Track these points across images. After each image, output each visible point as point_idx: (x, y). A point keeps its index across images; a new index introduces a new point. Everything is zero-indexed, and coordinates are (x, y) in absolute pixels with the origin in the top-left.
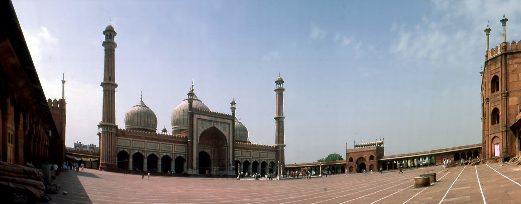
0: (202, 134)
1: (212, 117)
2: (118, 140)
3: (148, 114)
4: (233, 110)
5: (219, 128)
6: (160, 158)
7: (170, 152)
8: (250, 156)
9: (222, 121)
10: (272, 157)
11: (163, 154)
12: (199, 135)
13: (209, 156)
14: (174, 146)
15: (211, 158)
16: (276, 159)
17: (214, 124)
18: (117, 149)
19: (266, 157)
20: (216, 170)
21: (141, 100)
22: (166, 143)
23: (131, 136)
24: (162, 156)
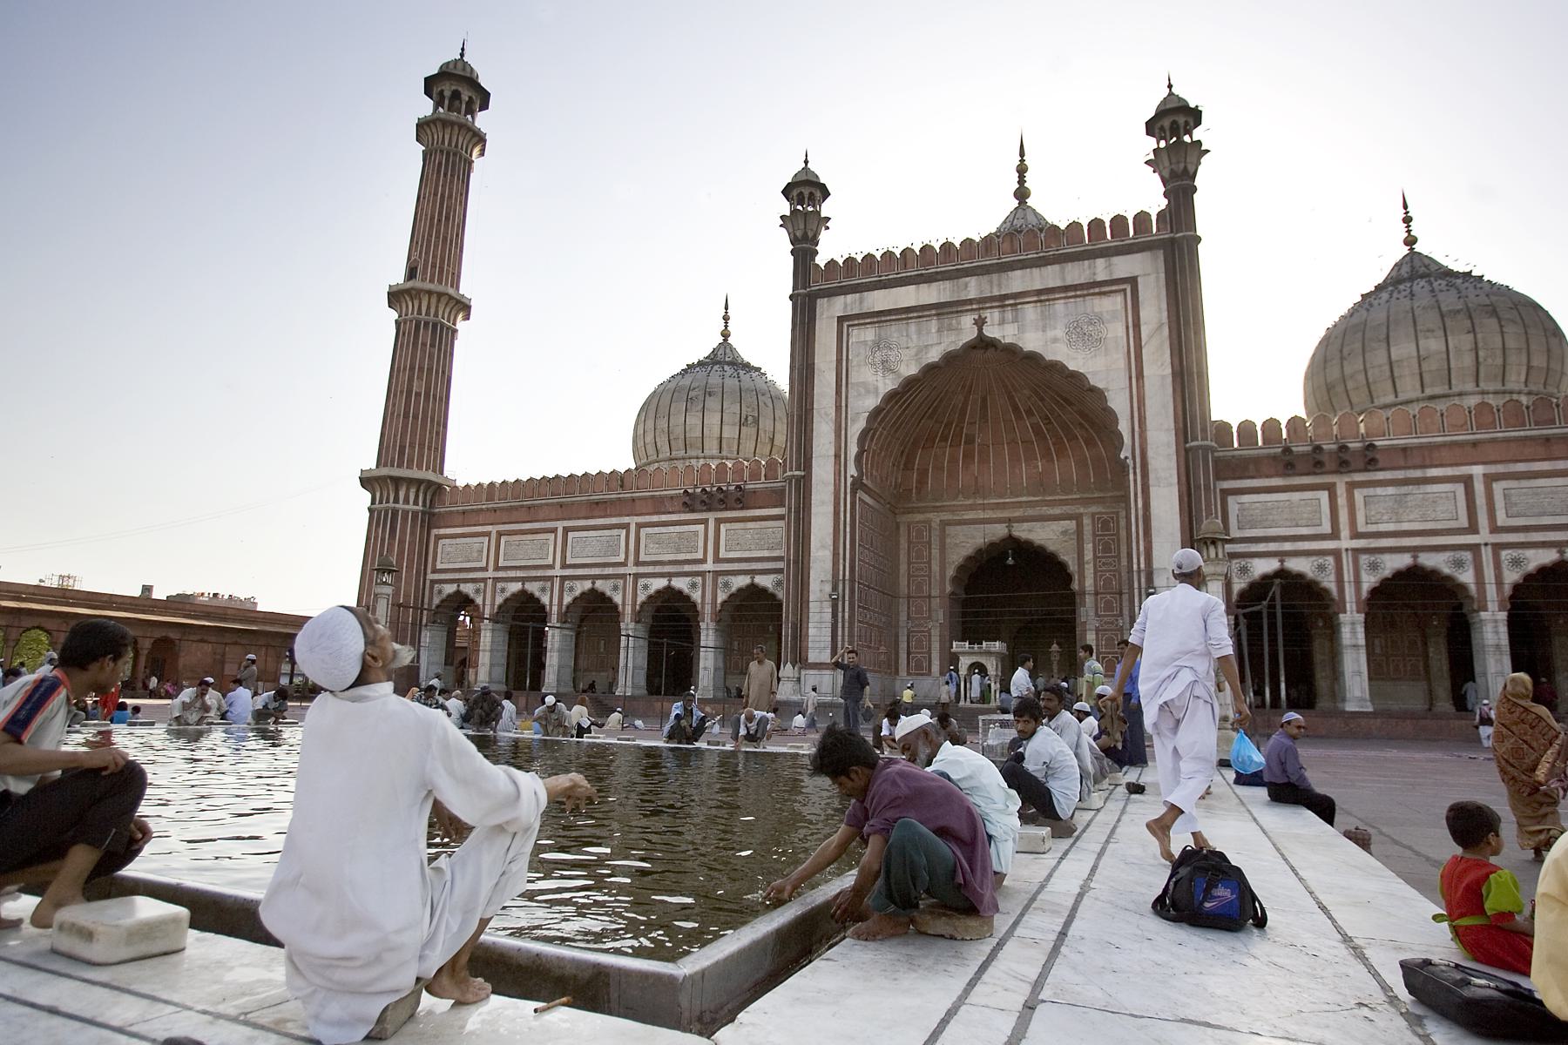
0: (875, 414)
2: (441, 542)
3: (692, 394)
5: (1031, 342)
7: (687, 568)
8: (1464, 522)
9: (1050, 286)
11: (646, 587)
12: (856, 428)
13: (1061, 567)
15: (1075, 586)
17: (980, 323)
18: (432, 588)
22: (664, 518)
23: (496, 516)
24: (641, 598)
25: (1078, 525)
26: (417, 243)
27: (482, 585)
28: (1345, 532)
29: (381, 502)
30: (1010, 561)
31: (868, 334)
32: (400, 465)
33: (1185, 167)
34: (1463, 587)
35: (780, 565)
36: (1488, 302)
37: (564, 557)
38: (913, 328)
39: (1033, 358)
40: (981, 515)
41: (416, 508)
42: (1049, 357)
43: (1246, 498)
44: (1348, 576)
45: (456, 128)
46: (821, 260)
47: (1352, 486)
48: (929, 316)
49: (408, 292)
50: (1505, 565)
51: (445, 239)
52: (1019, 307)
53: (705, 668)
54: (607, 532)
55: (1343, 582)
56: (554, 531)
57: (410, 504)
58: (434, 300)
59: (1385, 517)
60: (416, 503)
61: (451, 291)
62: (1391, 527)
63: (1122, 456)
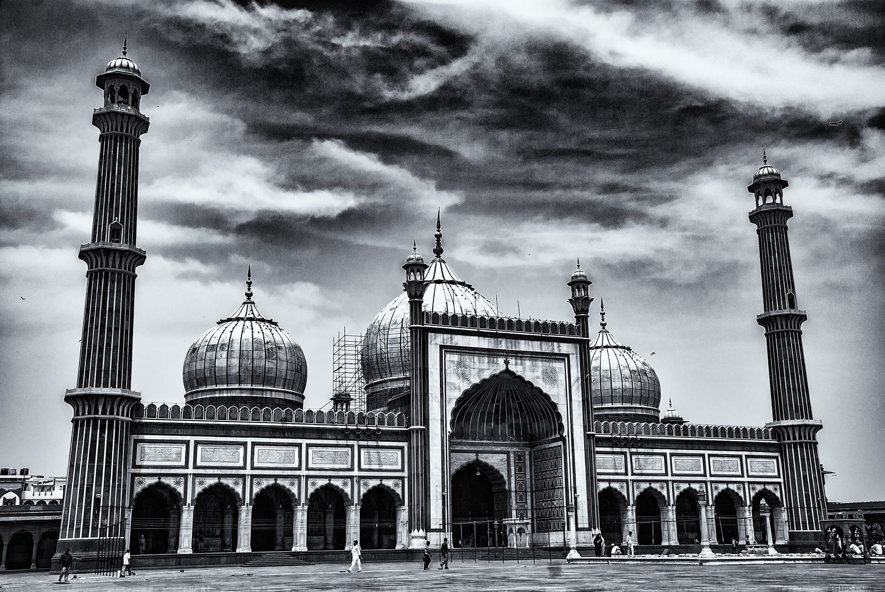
0: (460, 401)
1: (500, 339)
4: (581, 306)
5: (528, 376)
8: (663, 471)
9: (538, 350)
10: (761, 474)
11: (313, 484)
12: (451, 406)
13: (502, 477)
16: (781, 480)
17: (507, 363)
21: (249, 299)
24: (311, 490)
25: (507, 456)
26: (117, 209)
27: (182, 479)
29: (104, 413)
30: (478, 474)
31: (455, 357)
34: (664, 497)
38: (476, 358)
39: (530, 383)
40: (465, 448)
41: (127, 419)
42: (535, 385)
45: (142, 123)
47: (632, 454)
50: (675, 488)
53: (355, 533)
58: (134, 260)
60: (127, 416)
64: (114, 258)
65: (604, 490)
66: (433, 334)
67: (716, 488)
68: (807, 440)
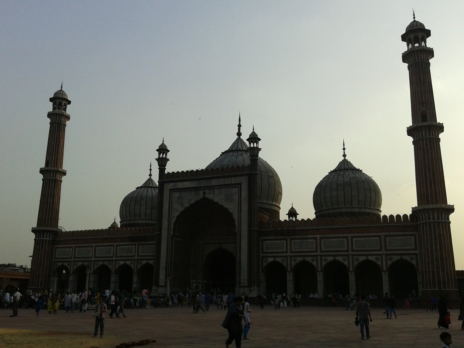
0: (178, 217)
2: (57, 250)
5: (216, 199)
6: (113, 272)
7: (130, 258)
8: (315, 249)
10: (399, 248)
11: (118, 264)
12: (174, 220)
14: (137, 245)
17: (204, 193)
19: (376, 248)
20: (197, 286)
21: (150, 177)
22: (124, 243)
24: (117, 267)
27: (70, 263)
28: (289, 251)
29: (38, 238)
31: (177, 194)
32: (44, 226)
33: (254, 154)
34: (314, 266)
35: (153, 258)
36: (349, 182)
37: (95, 254)
39: (217, 203)
41: (50, 239)
42: (220, 203)
43: (268, 242)
44: (289, 263)
46: (166, 173)
47: (291, 239)
48: (192, 190)
49: (47, 170)
51: (58, 152)
52: (214, 189)
54: (108, 247)
55: (288, 265)
56: (92, 246)
57: (48, 238)
59: (298, 248)
60: (49, 237)
61: (60, 170)
62: (299, 250)
63: (236, 231)
64: (53, 173)
65: (271, 262)
66: (166, 184)
67: (357, 259)
68: (432, 221)
